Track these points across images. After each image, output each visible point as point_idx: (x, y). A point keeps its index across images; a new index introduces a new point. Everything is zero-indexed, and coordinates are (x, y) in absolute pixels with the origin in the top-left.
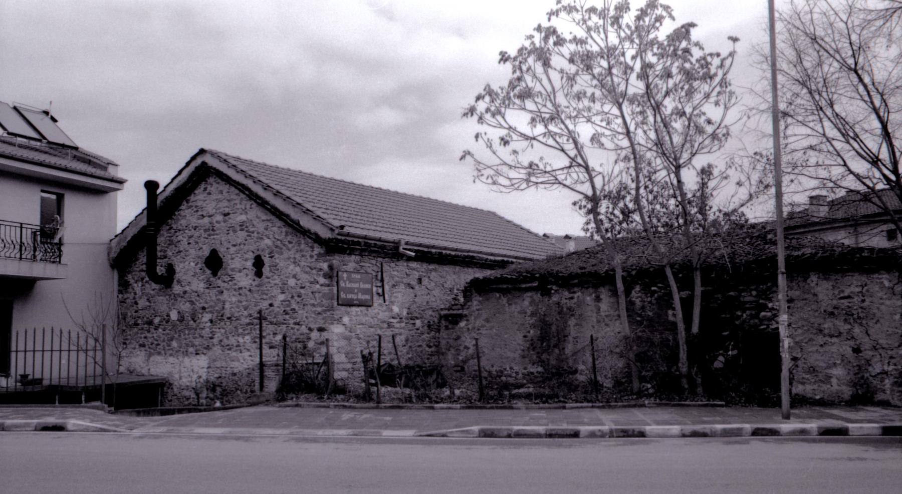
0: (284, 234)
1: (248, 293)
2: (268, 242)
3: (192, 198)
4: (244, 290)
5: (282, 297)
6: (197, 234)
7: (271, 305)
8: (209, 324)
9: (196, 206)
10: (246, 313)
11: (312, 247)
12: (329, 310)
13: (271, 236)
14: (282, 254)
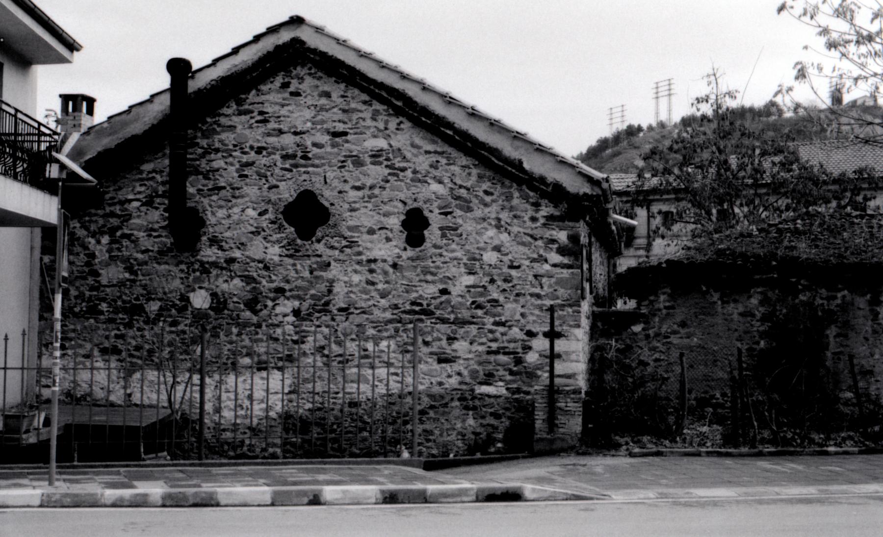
0: (474, 178)
1: (391, 270)
2: (435, 187)
3: (252, 96)
4: (380, 264)
5: (470, 280)
6: (263, 160)
7: (444, 292)
8: (291, 318)
9: (261, 113)
10: (383, 302)
11: (536, 205)
12: (570, 306)
13: (446, 180)
14: (469, 209)
